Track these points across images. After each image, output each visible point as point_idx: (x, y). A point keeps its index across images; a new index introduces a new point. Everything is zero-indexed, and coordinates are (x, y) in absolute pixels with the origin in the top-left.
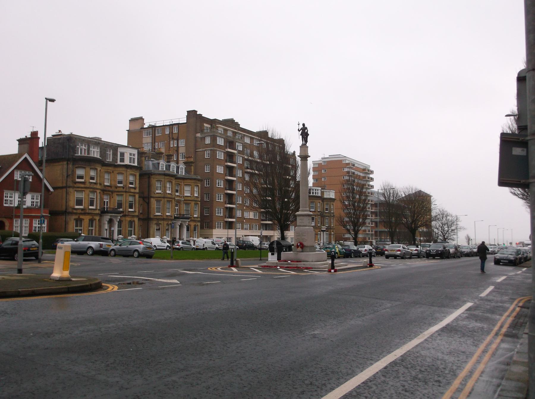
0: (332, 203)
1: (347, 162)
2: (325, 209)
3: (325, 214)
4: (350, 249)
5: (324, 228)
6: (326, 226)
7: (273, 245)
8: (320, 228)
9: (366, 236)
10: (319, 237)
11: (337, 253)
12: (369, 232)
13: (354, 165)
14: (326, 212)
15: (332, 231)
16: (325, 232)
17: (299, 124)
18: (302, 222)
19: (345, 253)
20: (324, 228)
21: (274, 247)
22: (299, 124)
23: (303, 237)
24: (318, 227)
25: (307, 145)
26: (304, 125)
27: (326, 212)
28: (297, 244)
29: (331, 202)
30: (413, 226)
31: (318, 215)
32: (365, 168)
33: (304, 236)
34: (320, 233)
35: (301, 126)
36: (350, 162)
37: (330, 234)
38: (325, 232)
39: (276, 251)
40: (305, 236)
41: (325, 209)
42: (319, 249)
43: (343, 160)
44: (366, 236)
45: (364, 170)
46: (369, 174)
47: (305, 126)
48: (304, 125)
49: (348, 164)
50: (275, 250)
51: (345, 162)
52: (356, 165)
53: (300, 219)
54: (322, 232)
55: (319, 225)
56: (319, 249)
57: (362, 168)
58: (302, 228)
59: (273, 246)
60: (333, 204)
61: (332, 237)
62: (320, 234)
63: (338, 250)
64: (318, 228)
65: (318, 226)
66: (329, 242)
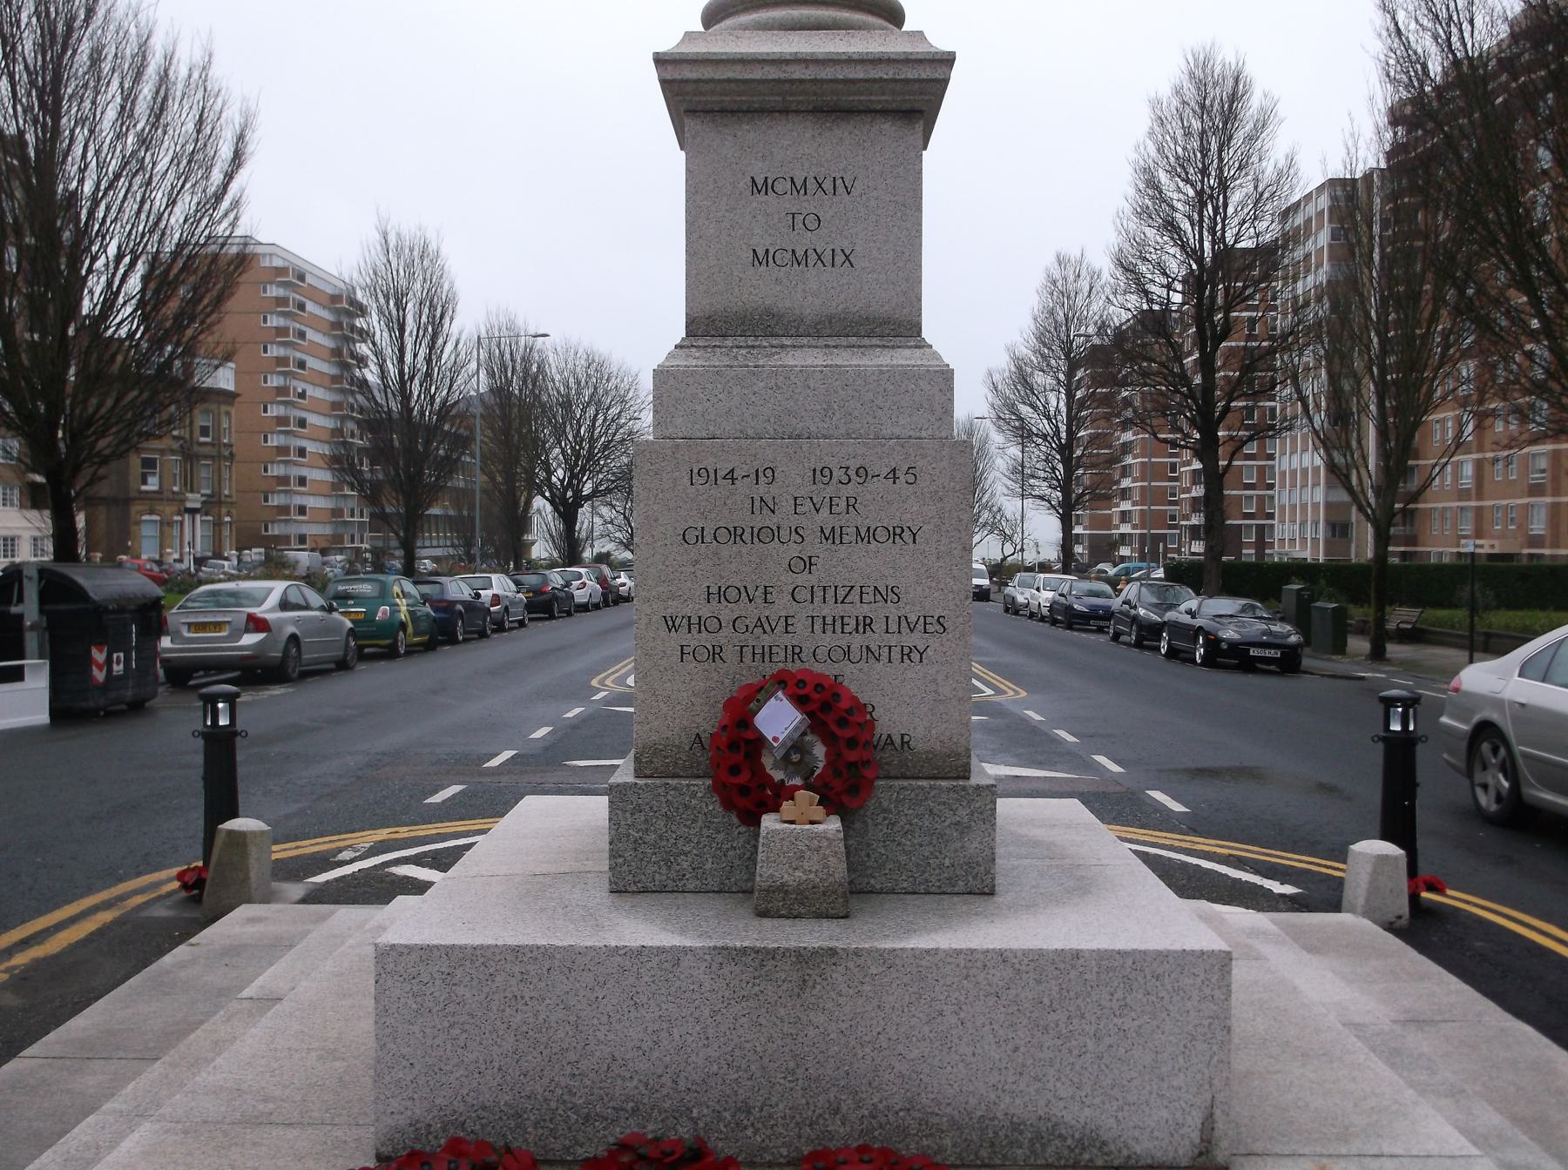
0: (224, 408)
1: (278, 263)
2: (197, 431)
3: (196, 449)
4: (446, 601)
5: (194, 501)
6: (203, 491)
7: (10, 603)
8: (178, 499)
9: (341, 530)
10: (176, 531)
11: (403, 626)
12: (352, 516)
13: (302, 277)
14: (202, 439)
15: (224, 510)
16: (198, 517)
18: (803, 241)
19: (435, 620)
20: (194, 501)
21: (20, 617)
23: (838, 564)
24: (171, 496)
27: (202, 439)
28: (707, 720)
29: (219, 403)
30: (569, 494)
31: (173, 452)
32: (337, 292)
33: (868, 536)
34: (179, 518)
36: (286, 264)
37: (218, 524)
38: (198, 517)
39: (41, 647)
40: (895, 534)
41: (197, 431)
42: (322, 608)
43: (264, 255)
44: (341, 530)
45: (335, 298)
46: (351, 315)
49: (281, 271)
50: (31, 641)
51: (271, 262)
52: (309, 279)
53: (762, 187)
54: (186, 516)
55: (176, 489)
56: (322, 608)
57: (330, 291)
58: (807, 358)
59: (14, 610)
60: (228, 414)
61: (226, 532)
62: (182, 523)
63: (404, 608)
64: (173, 500)
65: (174, 493)
66: (214, 553)
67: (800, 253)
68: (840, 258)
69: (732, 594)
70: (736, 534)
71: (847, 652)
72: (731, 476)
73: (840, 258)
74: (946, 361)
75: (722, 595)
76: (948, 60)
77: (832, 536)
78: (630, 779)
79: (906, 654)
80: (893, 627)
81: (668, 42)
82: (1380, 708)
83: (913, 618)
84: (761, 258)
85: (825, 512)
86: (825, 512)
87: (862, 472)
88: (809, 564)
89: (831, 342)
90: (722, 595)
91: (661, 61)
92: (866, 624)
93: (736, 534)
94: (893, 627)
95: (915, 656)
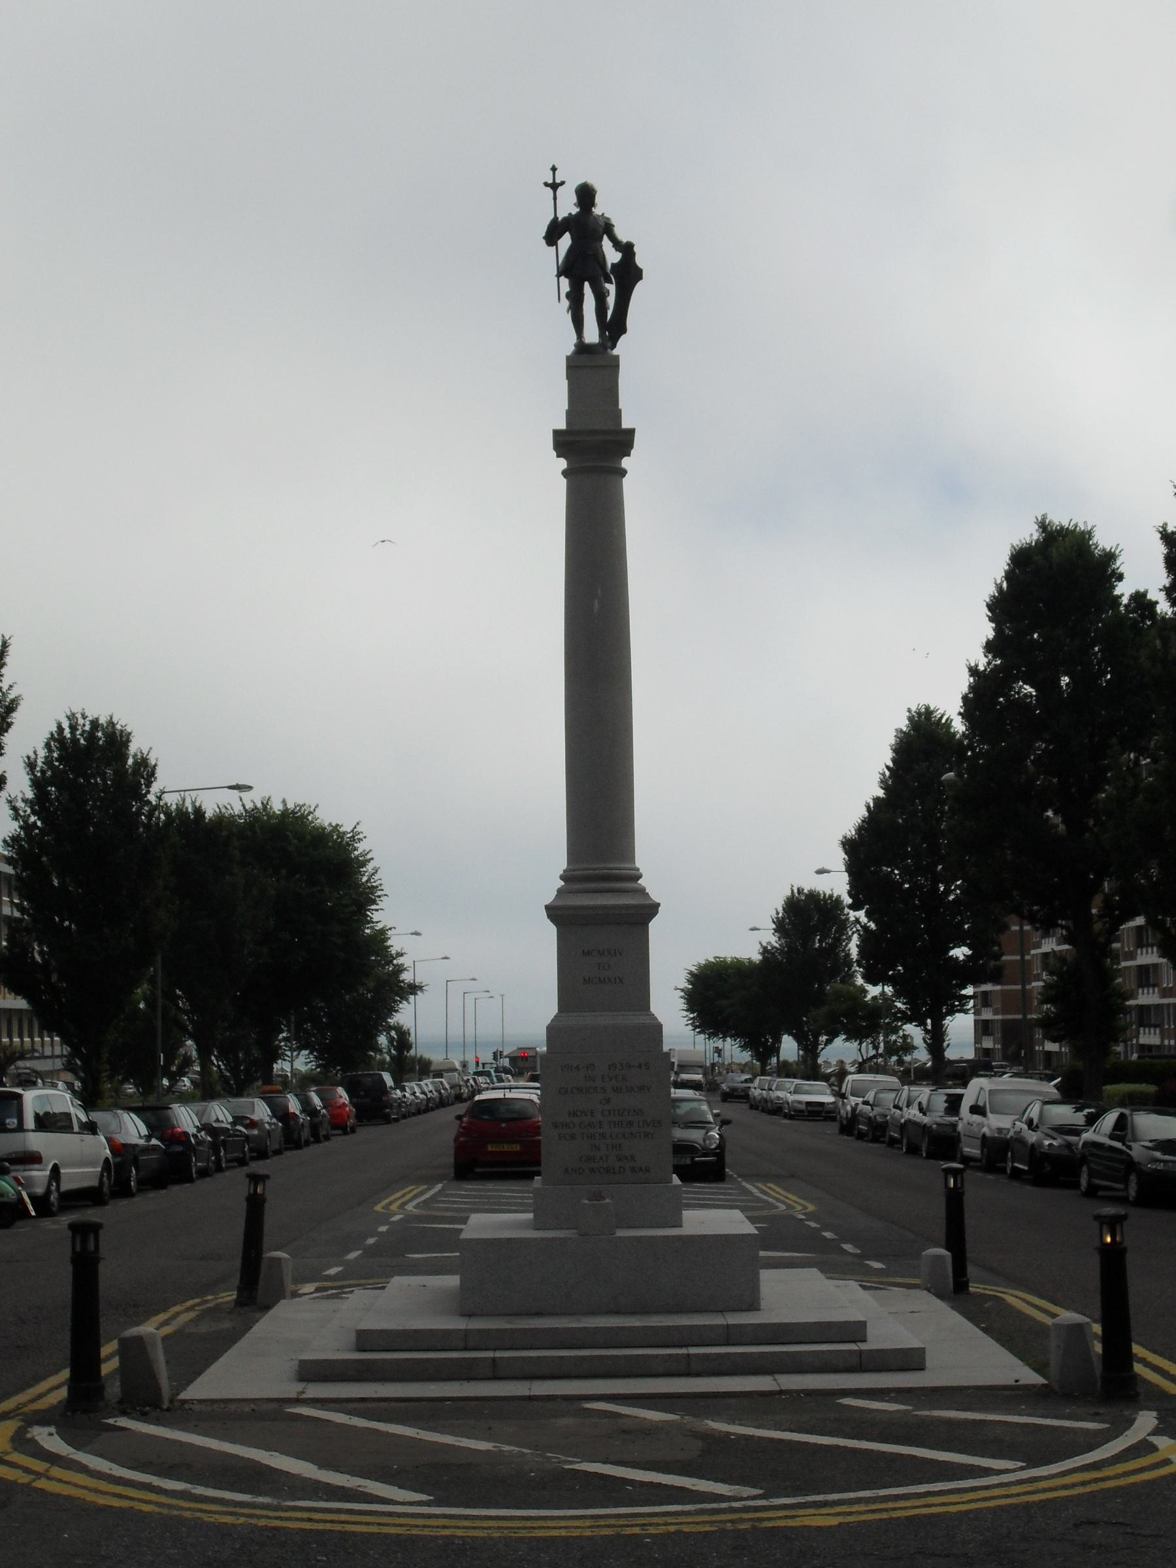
17: (554, 186)
22: (554, 186)
25: (623, 348)
26: (586, 195)
35: (568, 206)
40: (641, 1088)
47: (597, 211)
48: (586, 195)
67: (602, 979)
68: (618, 981)
69: (579, 1113)
70: (580, 1090)
71: (624, 1135)
72: (577, 1068)
73: (618, 981)
74: (660, 1020)
75: (574, 1114)
76: (659, 905)
77: (617, 1090)
78: (540, 1186)
79: (647, 1135)
80: (641, 1124)
81: (550, 897)
82: (943, 1174)
83: (648, 1121)
84: (587, 981)
85: (614, 1081)
86: (614, 1081)
87: (629, 1066)
88: (608, 1101)
89: (615, 1013)
90: (574, 1114)
91: (547, 908)
92: (630, 1124)
93: (580, 1090)
94: (641, 1124)
95: (650, 1136)
